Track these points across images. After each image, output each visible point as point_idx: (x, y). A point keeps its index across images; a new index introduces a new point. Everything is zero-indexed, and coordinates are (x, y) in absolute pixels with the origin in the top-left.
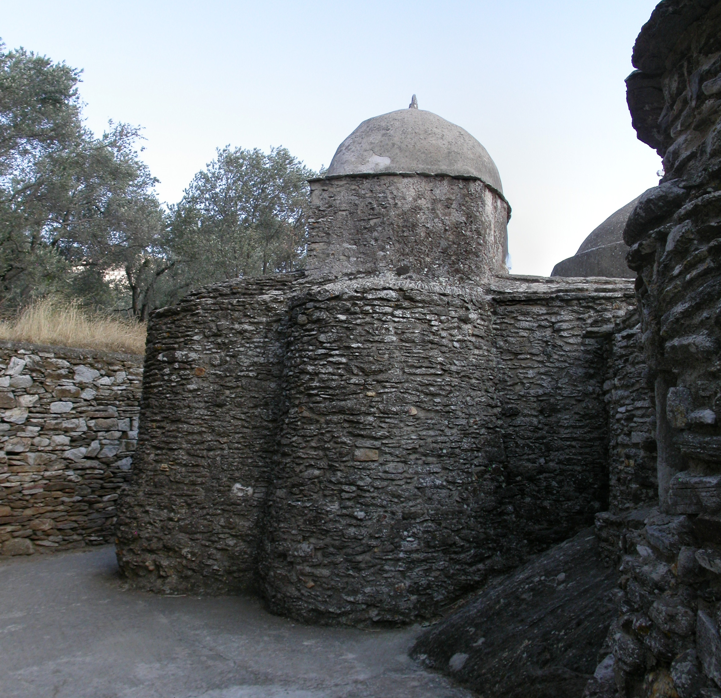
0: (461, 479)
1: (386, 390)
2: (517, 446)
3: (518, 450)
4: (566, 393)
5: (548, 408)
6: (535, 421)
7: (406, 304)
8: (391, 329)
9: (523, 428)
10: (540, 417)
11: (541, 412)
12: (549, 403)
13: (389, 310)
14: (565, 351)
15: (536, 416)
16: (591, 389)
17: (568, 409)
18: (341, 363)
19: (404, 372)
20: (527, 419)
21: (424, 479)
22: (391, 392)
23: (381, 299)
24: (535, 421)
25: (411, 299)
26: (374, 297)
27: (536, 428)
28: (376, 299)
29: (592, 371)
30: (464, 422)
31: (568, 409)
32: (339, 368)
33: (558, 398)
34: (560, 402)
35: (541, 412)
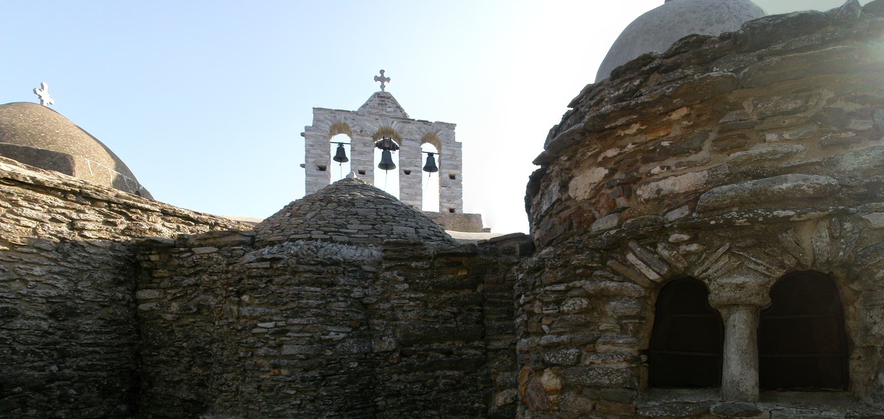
4: (89, 298)
5: (61, 311)
9: (25, 332)
10: (50, 321)
11: (53, 315)
12: (66, 306)
15: (44, 319)
16: (120, 295)
17: (89, 314)
20: (34, 323)
24: (44, 325)
27: (46, 332)
29: (122, 278)
31: (89, 314)
33: (77, 301)
34: (80, 306)
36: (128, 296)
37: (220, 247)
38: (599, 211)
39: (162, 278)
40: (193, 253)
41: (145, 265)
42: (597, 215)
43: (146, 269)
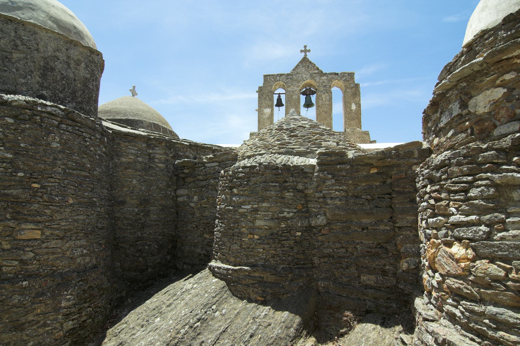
0: (97, 248)
1: (50, 184)
2: (124, 225)
3: (124, 227)
6: (136, 210)
7: (70, 122)
8: (57, 138)
13: (57, 123)
14: (156, 170)
15: (136, 208)
18: (7, 158)
19: (65, 172)
21: (75, 251)
22: (54, 186)
23: (50, 113)
25: (73, 120)
26: (44, 110)
28: (44, 112)
30: (99, 209)
32: (4, 162)
35: (141, 204)
36: (173, 193)
37: (219, 163)
38: (499, 121)
39: (190, 183)
40: (206, 167)
41: (182, 175)
42: (498, 123)
43: (182, 178)
